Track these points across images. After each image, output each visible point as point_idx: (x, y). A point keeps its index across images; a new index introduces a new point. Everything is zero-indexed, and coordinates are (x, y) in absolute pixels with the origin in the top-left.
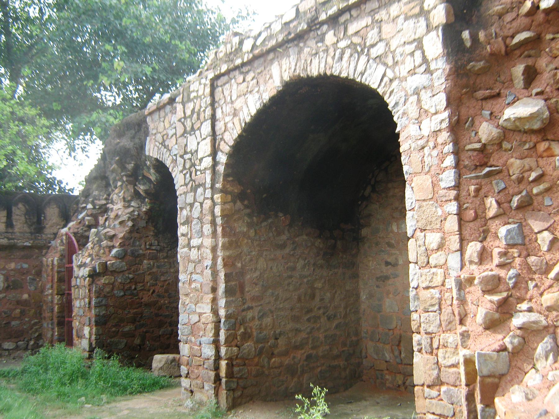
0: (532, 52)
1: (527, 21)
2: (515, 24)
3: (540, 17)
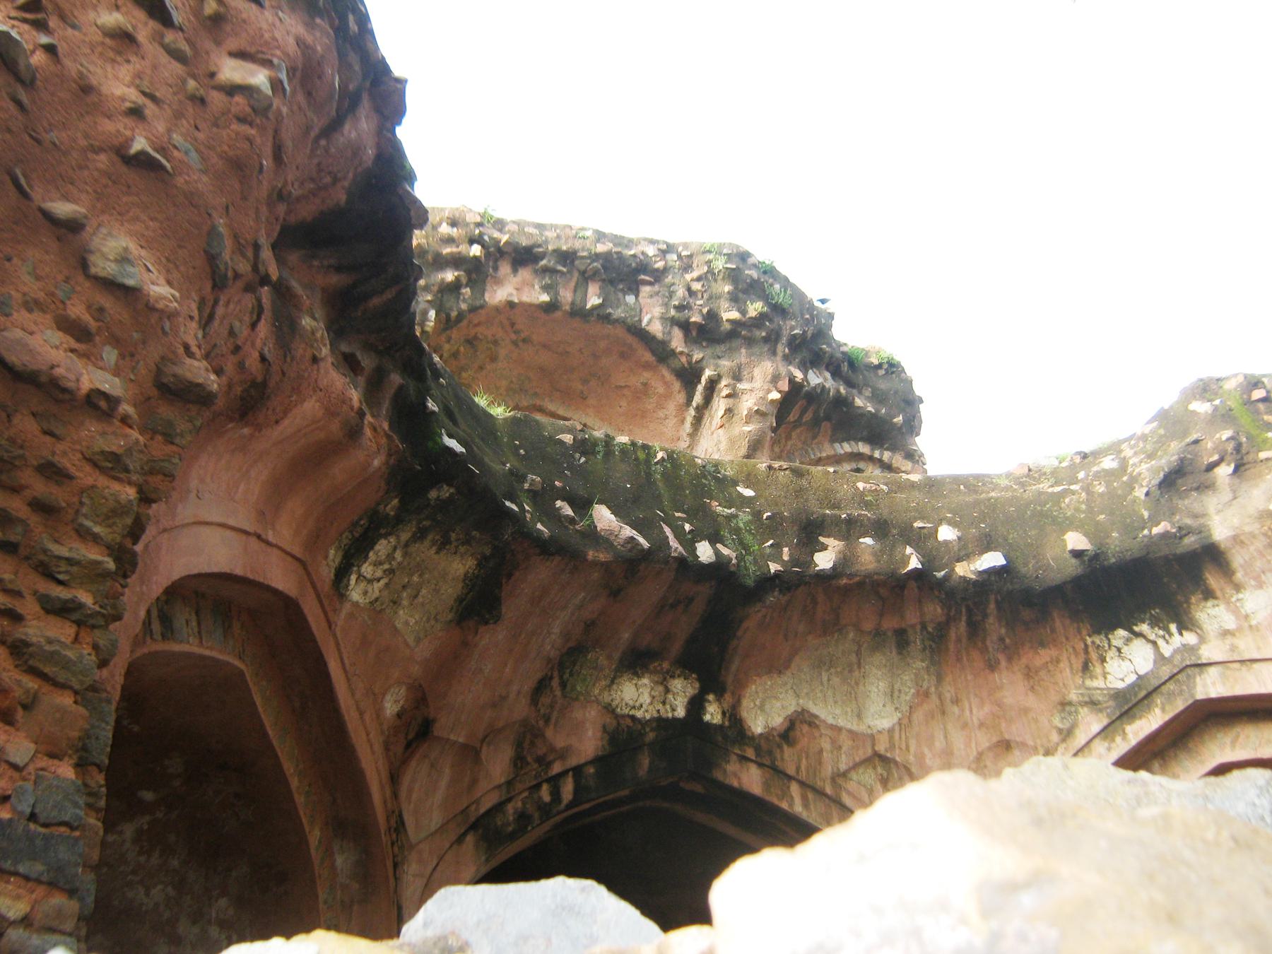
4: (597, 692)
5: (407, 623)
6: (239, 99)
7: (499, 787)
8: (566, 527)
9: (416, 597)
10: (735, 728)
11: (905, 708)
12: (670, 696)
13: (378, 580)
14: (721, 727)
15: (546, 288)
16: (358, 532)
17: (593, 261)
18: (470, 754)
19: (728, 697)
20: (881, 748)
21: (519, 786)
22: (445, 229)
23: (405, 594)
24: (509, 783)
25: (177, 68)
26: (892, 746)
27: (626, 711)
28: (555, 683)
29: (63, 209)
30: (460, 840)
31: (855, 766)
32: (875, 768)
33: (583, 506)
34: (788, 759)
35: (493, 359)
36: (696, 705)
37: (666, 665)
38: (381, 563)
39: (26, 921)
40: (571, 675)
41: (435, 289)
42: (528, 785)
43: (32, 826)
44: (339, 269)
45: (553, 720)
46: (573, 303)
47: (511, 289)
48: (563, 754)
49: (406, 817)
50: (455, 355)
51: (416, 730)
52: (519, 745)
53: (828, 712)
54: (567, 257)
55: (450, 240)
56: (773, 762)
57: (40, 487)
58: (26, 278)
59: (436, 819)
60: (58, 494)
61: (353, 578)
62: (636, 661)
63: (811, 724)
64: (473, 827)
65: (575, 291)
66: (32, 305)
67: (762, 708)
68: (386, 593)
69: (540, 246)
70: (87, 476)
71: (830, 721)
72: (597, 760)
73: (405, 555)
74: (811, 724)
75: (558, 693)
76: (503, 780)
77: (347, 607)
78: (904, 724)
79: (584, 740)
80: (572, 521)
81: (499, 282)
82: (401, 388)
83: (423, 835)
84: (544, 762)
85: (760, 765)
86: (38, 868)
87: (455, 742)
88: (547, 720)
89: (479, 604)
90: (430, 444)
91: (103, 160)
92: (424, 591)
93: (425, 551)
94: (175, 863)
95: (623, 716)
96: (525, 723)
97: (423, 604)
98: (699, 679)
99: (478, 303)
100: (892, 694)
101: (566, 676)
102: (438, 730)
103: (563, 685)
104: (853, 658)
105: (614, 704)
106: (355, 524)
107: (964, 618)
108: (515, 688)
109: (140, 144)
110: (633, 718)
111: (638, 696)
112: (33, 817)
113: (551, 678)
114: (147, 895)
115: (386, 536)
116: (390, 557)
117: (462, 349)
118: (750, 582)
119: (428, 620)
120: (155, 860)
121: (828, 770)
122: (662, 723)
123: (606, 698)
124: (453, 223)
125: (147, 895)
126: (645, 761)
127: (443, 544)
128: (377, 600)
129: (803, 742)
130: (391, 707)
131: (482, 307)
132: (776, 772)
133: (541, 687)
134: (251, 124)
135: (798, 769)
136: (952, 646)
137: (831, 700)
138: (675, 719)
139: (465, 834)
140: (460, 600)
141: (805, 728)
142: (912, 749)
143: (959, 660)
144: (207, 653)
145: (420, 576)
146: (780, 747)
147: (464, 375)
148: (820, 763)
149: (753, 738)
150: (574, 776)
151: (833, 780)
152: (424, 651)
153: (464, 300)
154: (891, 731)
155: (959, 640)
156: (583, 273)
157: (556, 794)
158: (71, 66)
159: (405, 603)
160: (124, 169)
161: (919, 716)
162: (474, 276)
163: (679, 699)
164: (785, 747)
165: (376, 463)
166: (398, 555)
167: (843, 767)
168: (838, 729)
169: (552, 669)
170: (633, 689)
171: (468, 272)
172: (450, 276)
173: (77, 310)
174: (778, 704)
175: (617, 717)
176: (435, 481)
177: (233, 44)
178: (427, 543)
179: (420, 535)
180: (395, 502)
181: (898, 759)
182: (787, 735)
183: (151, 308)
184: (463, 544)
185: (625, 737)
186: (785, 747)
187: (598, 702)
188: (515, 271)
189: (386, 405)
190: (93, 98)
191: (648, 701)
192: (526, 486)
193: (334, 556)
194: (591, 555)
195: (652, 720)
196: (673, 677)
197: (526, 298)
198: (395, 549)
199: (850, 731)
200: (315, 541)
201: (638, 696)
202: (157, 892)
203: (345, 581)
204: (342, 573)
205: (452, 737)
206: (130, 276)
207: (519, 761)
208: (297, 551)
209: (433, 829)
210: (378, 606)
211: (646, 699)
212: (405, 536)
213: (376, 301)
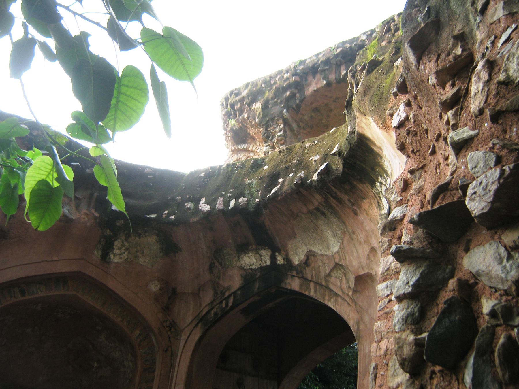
4: (235, 263)
5: (145, 262)
7: (208, 304)
9: (143, 253)
10: (289, 264)
11: (340, 241)
12: (263, 257)
13: (124, 253)
14: (284, 265)
15: (324, 79)
17: (337, 57)
18: (196, 295)
19: (282, 252)
20: (337, 260)
21: (215, 303)
22: (286, 75)
23: (138, 254)
24: (212, 303)
26: (340, 260)
27: (248, 267)
28: (217, 264)
30: (196, 325)
31: (332, 270)
32: (340, 270)
33: (197, 202)
34: (308, 273)
35: (331, 110)
36: (273, 259)
37: (254, 247)
40: (222, 260)
41: (284, 100)
42: (218, 302)
45: (221, 277)
46: (336, 79)
47: (315, 84)
48: (228, 289)
50: (311, 117)
52: (214, 288)
53: (317, 249)
54: (327, 62)
55: (288, 79)
56: (303, 275)
61: (112, 256)
62: (243, 248)
63: (314, 256)
65: (336, 73)
67: (296, 253)
69: (316, 63)
71: (320, 253)
72: (240, 288)
73: (128, 243)
74: (314, 256)
75: (220, 267)
78: (342, 248)
79: (235, 282)
81: (309, 85)
83: (186, 325)
84: (223, 293)
85: (299, 278)
88: (219, 278)
92: (145, 250)
95: (247, 269)
98: (269, 248)
99: (303, 97)
100: (335, 235)
101: (220, 261)
103: (221, 264)
104: (312, 224)
105: (243, 266)
107: (330, 196)
110: (251, 269)
111: (251, 261)
113: (214, 263)
115: (116, 240)
116: (123, 245)
117: (313, 114)
118: (252, 209)
119: (153, 258)
121: (323, 275)
122: (262, 268)
123: (239, 264)
124: (287, 72)
126: (257, 285)
128: (127, 259)
129: (313, 264)
130: (154, 287)
131: (305, 98)
132: (305, 281)
133: (211, 268)
135: (312, 276)
136: (338, 209)
137: (317, 243)
138: (267, 266)
141: (312, 257)
142: (347, 259)
143: (345, 214)
145: (140, 246)
146: (305, 268)
147: (323, 122)
148: (320, 272)
149: (295, 267)
150: (234, 297)
151: (325, 278)
153: (297, 99)
154: (338, 252)
155: (338, 206)
156: (337, 64)
157: (227, 304)
161: (345, 242)
162: (299, 88)
163: (266, 258)
164: (307, 268)
166: (125, 243)
167: (327, 272)
168: (322, 255)
169: (213, 260)
170: (248, 258)
171: (296, 88)
172: (288, 93)
174: (301, 250)
175: (245, 270)
179: (128, 236)
180: (108, 230)
181: (343, 264)
182: (306, 263)
185: (249, 277)
186: (307, 268)
187: (237, 267)
188: (314, 77)
189: (93, 204)
191: (255, 261)
193: (97, 254)
194: (192, 220)
195: (259, 268)
196: (259, 250)
197: (319, 86)
198: (123, 242)
199: (326, 255)
201: (251, 261)
203: (108, 258)
204: (105, 257)
205: (186, 291)
207: (215, 294)
209: (189, 322)
211: (254, 261)
212: (123, 238)
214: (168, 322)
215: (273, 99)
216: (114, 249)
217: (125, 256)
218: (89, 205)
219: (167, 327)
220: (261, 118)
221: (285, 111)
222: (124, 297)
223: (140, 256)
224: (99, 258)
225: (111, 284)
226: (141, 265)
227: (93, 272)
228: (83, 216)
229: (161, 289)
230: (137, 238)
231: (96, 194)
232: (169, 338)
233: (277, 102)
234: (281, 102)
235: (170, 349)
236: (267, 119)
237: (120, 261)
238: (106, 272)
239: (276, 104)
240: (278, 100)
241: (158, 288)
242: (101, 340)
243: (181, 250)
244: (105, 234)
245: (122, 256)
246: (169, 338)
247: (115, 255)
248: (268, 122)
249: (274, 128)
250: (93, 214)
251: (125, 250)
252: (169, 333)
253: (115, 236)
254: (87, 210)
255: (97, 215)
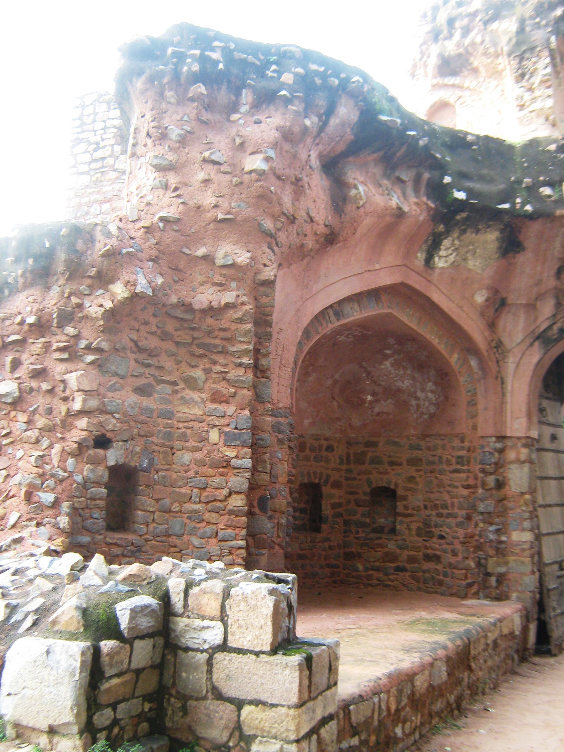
0: (20, 349)
1: (18, 328)
2: (11, 328)
3: (26, 328)
5: (475, 265)
6: (253, 175)
7: (548, 319)
8: (546, 201)
9: (475, 254)
13: (451, 254)
16: (430, 243)
18: (531, 307)
23: (468, 255)
24: (554, 316)
25: (228, 177)
29: (202, 251)
30: (532, 345)
38: (449, 248)
39: (237, 457)
41: (552, 23)
43: (236, 431)
44: (374, 152)
49: (503, 339)
51: (498, 304)
57: (222, 334)
58: (199, 277)
59: (519, 337)
60: (228, 335)
61: (436, 259)
64: (537, 338)
66: (202, 284)
68: (458, 258)
70: (234, 326)
73: (460, 241)
76: (549, 315)
77: (437, 272)
80: (549, 196)
82: (429, 179)
83: (514, 345)
86: (238, 443)
87: (521, 304)
89: (511, 245)
90: (448, 199)
91: (212, 226)
92: (478, 251)
93: (470, 236)
94: (409, 372)
96: (556, 288)
97: (480, 256)
102: (510, 301)
106: (426, 241)
108: (545, 275)
109: (220, 216)
112: (236, 428)
114: (403, 383)
115: (445, 238)
116: (453, 244)
119: (486, 261)
120: (401, 372)
125: (403, 383)
127: (478, 231)
128: (454, 262)
130: (480, 298)
134: (260, 181)
139: (534, 341)
140: (500, 248)
144: (365, 315)
152: (489, 272)
158: (191, 203)
159: (470, 258)
160: (220, 224)
165: (421, 218)
166: (457, 242)
173: (217, 278)
176: (457, 212)
177: (249, 151)
178: (468, 234)
179: (464, 232)
180: (442, 226)
183: (240, 267)
184: (488, 228)
189: (423, 189)
190: (201, 209)
192: (524, 185)
193: (421, 256)
198: (453, 241)
200: (409, 254)
202: (406, 382)
203: (432, 262)
206: (229, 260)
208: (399, 262)
209: (519, 340)
210: (456, 264)
212: (456, 235)
213: (399, 154)
214: (495, 342)
215: (532, 18)
216: (440, 250)
217: (452, 258)
218: (416, 190)
219: (495, 347)
220: (514, 46)
221: (553, 39)
222: (450, 313)
223: (470, 258)
224: (423, 263)
225: (436, 297)
226: (469, 270)
227: (416, 282)
228: (414, 207)
229: (487, 300)
230: (474, 235)
231: (426, 175)
232: (498, 362)
233: (538, 23)
234: (547, 25)
235: (499, 376)
236: (524, 48)
237: (445, 265)
238: (429, 281)
239: (538, 26)
240: (542, 19)
241: (484, 298)
242: (383, 367)
243: (524, 249)
244: (436, 230)
245: (448, 259)
246: (498, 362)
247: (440, 257)
248: (524, 52)
249: (535, 63)
250: (426, 204)
251: (453, 250)
252: (497, 355)
253: (447, 233)
254: (417, 197)
255: (433, 205)
